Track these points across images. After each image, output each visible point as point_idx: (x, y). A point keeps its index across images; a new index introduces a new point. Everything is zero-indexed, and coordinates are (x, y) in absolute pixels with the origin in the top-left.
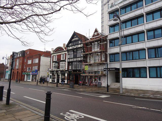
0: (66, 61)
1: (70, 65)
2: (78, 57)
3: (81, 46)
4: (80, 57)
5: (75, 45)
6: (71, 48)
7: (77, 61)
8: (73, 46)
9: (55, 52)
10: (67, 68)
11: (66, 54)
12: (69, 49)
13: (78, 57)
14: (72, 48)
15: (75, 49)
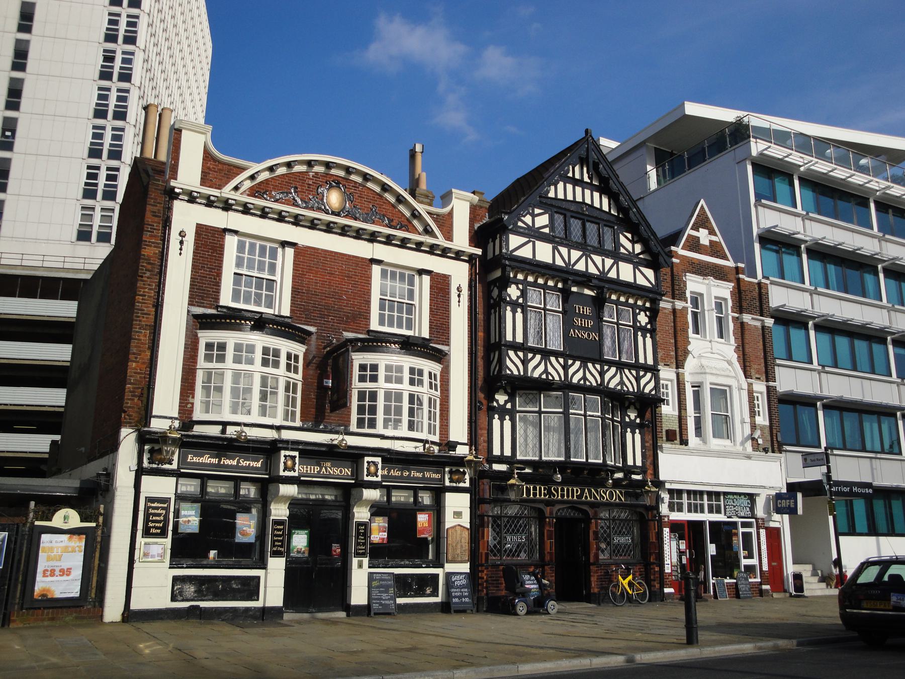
0: (440, 357)
1: (491, 411)
2: (611, 363)
3: (641, 281)
4: (630, 366)
5: (586, 249)
6: (544, 252)
7: (601, 390)
8: (571, 246)
9: (254, 192)
10: (459, 431)
11: (440, 285)
12: (526, 253)
13: (611, 363)
14: (559, 262)
15: (585, 279)
